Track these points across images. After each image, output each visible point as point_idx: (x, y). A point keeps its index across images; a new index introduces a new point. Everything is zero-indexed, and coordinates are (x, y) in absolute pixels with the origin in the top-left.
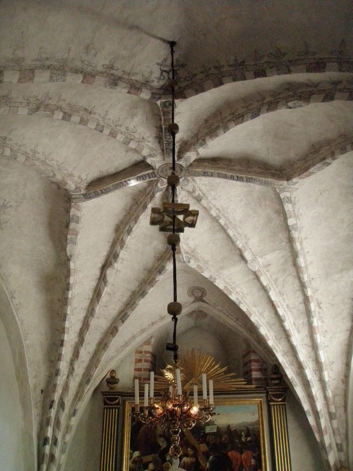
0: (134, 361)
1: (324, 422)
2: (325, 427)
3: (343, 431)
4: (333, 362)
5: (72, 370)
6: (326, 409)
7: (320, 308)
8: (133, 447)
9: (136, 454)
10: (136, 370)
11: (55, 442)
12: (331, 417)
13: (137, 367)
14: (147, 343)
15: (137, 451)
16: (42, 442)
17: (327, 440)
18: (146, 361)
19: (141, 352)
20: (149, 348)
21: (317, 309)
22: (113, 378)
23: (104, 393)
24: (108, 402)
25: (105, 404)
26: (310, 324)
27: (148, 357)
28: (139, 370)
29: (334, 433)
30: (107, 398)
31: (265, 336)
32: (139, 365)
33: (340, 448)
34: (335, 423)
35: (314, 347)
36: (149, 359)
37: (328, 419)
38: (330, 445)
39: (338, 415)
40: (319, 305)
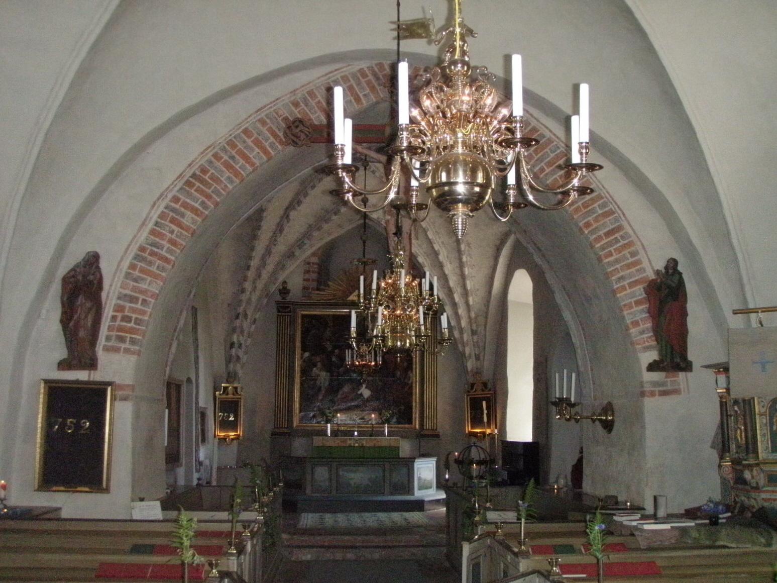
0: (303, 271)
1: (465, 337)
2: (467, 340)
3: (481, 344)
4: (478, 290)
5: (254, 288)
6: (469, 326)
7: (469, 247)
8: (304, 349)
9: (307, 354)
10: (304, 280)
11: (240, 346)
12: (474, 333)
13: (305, 278)
14: (313, 254)
15: (307, 352)
16: (228, 346)
17: (467, 350)
18: (313, 272)
19: (309, 263)
20: (315, 260)
21: (467, 248)
22: (285, 288)
23: (277, 303)
24: (281, 310)
25: (279, 311)
26: (460, 260)
27: (315, 268)
28: (307, 280)
29: (474, 345)
30: (281, 306)
31: (422, 264)
32: (307, 276)
33: (477, 358)
34: (475, 338)
35: (463, 277)
36: (316, 270)
37: (470, 334)
38: (470, 354)
39: (479, 331)
40: (469, 245)
